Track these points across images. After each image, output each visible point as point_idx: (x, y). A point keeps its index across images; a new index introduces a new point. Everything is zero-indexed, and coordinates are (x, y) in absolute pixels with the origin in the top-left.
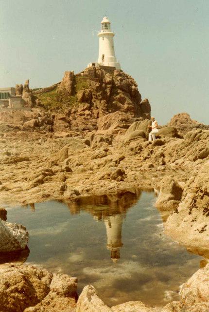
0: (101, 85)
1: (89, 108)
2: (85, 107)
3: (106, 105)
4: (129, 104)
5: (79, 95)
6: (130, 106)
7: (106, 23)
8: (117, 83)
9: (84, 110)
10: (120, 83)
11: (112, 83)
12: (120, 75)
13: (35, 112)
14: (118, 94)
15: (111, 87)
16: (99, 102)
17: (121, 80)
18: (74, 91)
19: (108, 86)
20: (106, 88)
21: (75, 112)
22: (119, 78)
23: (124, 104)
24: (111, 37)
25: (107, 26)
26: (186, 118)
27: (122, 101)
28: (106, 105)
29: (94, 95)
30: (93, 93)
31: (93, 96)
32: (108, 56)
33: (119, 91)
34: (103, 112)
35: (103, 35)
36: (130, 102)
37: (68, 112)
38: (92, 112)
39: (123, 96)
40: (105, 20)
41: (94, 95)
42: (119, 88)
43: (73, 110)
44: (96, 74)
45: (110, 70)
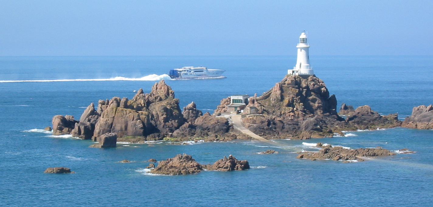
0: (299, 91)
1: (293, 111)
2: (290, 110)
3: (303, 107)
4: (319, 103)
5: (286, 101)
6: (320, 105)
7: (303, 39)
8: (311, 87)
9: (289, 112)
10: (313, 87)
11: (307, 87)
12: (313, 80)
13: (266, 118)
14: (312, 95)
15: (306, 91)
16: (298, 105)
17: (314, 85)
18: (282, 99)
19: (304, 90)
20: (303, 91)
21: (284, 114)
22: (312, 83)
23: (315, 103)
24: (307, 49)
25: (304, 41)
26: (367, 111)
27: (314, 101)
28: (303, 107)
29: (295, 100)
30: (294, 99)
31: (295, 101)
32: (304, 64)
33: (312, 93)
34: (302, 113)
35: (301, 49)
36: (320, 102)
37: (280, 114)
38: (294, 113)
39: (315, 97)
40: (303, 36)
41: (295, 100)
42: (313, 91)
43: (282, 113)
44: (296, 82)
45: (305, 77)
